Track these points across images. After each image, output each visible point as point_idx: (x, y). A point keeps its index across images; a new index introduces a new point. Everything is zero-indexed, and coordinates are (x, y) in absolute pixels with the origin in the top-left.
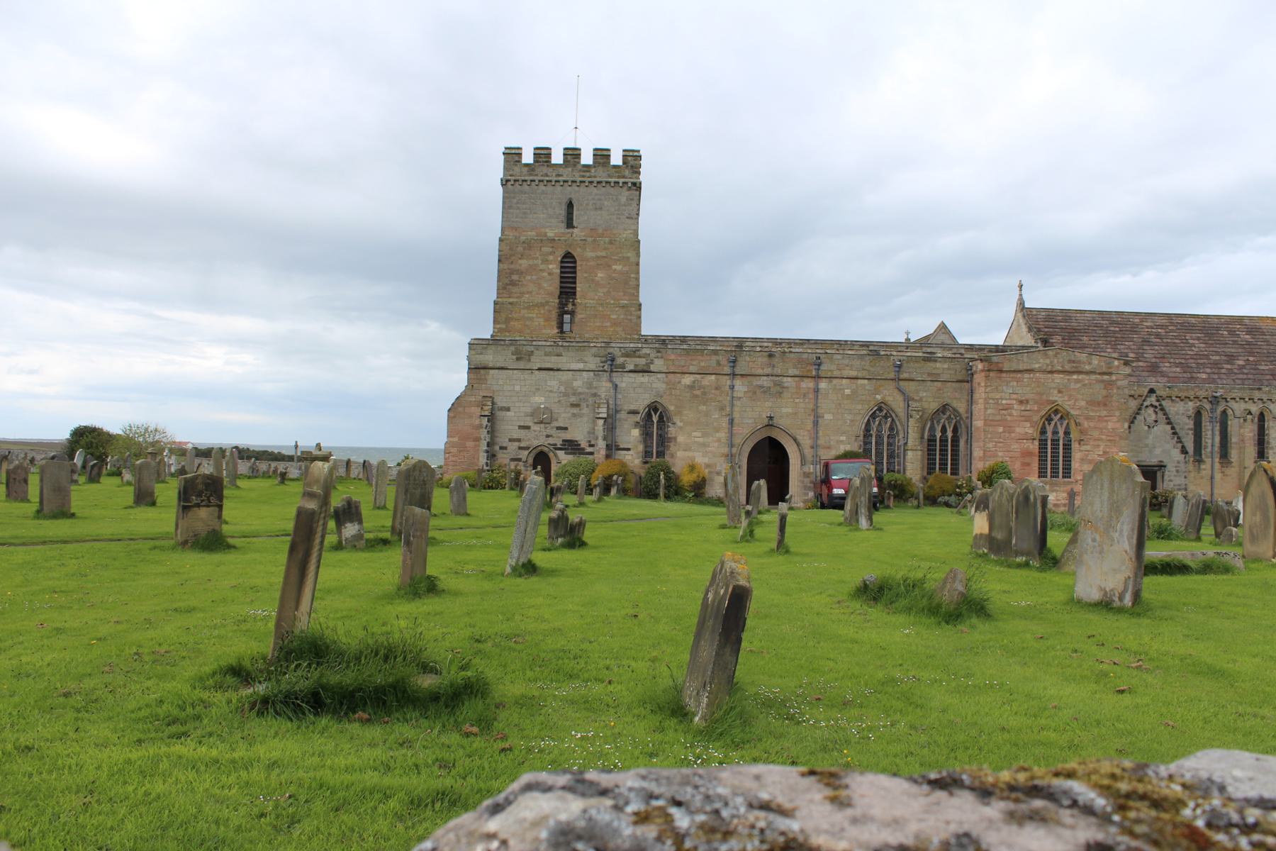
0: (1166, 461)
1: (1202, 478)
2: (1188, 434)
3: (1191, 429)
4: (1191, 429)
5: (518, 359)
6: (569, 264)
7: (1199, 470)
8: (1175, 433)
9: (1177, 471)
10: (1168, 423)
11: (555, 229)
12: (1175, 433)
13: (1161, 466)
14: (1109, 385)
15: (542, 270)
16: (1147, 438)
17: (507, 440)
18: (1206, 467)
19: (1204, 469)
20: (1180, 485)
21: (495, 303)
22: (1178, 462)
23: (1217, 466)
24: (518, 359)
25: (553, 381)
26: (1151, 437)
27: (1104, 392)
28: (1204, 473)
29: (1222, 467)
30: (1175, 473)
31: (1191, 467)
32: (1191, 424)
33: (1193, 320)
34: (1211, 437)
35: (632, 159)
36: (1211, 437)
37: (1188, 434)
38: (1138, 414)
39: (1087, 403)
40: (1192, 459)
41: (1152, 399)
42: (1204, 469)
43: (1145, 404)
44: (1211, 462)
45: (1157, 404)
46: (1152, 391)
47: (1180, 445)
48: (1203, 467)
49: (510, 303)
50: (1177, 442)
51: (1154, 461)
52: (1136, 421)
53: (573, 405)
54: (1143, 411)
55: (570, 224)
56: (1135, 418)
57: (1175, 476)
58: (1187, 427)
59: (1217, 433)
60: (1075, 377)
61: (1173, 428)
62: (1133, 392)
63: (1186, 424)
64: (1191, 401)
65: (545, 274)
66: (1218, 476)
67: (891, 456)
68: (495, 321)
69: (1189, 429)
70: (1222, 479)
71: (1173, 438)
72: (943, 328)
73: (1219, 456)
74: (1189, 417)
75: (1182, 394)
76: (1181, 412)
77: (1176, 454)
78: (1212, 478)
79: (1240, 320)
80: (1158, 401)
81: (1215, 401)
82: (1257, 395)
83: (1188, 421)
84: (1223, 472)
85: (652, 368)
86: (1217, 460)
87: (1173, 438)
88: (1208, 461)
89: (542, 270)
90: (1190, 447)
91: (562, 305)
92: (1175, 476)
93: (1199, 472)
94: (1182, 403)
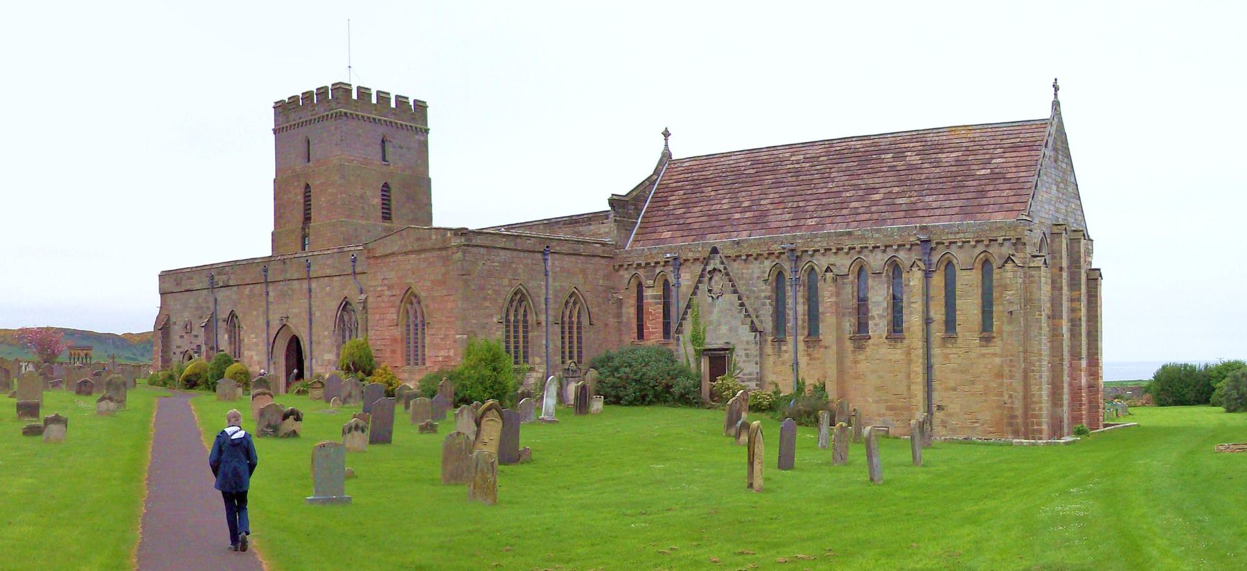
0: (733, 341)
1: (783, 363)
2: (764, 304)
3: (769, 298)
4: (769, 298)
7: (779, 353)
8: (742, 305)
9: (747, 355)
10: (735, 292)
12: (742, 305)
13: (729, 350)
14: (446, 260)
16: (711, 313)
17: (175, 347)
18: (788, 347)
19: (786, 352)
20: (750, 375)
22: (748, 343)
23: (801, 346)
26: (716, 310)
27: (443, 270)
28: (786, 356)
29: (808, 347)
30: (744, 358)
31: (769, 349)
32: (766, 290)
33: (858, 144)
34: (797, 307)
36: (797, 307)
37: (764, 304)
38: (699, 282)
39: (433, 282)
40: (770, 338)
41: (715, 263)
42: (786, 352)
43: (709, 268)
44: (795, 344)
45: (721, 267)
46: (715, 251)
47: (749, 320)
48: (784, 348)
50: (745, 316)
51: (719, 344)
52: (699, 293)
54: (706, 279)
56: (697, 287)
57: (744, 361)
58: (763, 295)
59: (800, 300)
60: (423, 256)
61: (740, 298)
62: (698, 255)
63: (763, 291)
64: (767, 258)
66: (803, 360)
67: (525, 347)
69: (766, 297)
70: (808, 364)
71: (740, 312)
73: (806, 332)
74: (765, 281)
75: (754, 252)
76: (756, 275)
77: (745, 334)
78: (796, 364)
80: (722, 263)
81: (795, 256)
82: (848, 243)
83: (764, 287)
84: (809, 355)
86: (801, 338)
87: (740, 312)
88: (790, 339)
90: (768, 324)
92: (744, 361)
93: (780, 356)
94: (757, 263)
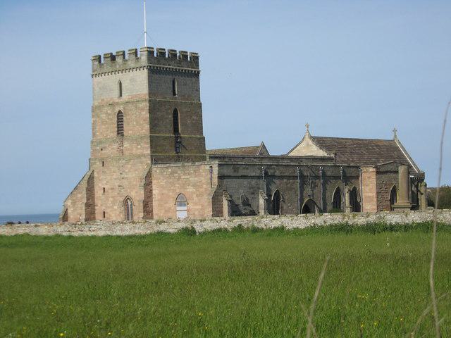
5: (235, 171)
6: (175, 113)
11: (169, 98)
15: (166, 118)
21: (151, 137)
24: (235, 171)
25: (245, 182)
35: (195, 58)
49: (157, 137)
53: (253, 193)
55: (174, 94)
65: (168, 121)
68: (151, 148)
72: (264, 147)
79: (371, 141)
85: (276, 174)
89: (166, 118)
91: (177, 138)
